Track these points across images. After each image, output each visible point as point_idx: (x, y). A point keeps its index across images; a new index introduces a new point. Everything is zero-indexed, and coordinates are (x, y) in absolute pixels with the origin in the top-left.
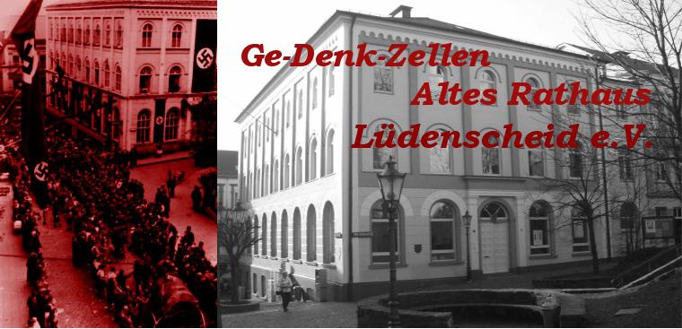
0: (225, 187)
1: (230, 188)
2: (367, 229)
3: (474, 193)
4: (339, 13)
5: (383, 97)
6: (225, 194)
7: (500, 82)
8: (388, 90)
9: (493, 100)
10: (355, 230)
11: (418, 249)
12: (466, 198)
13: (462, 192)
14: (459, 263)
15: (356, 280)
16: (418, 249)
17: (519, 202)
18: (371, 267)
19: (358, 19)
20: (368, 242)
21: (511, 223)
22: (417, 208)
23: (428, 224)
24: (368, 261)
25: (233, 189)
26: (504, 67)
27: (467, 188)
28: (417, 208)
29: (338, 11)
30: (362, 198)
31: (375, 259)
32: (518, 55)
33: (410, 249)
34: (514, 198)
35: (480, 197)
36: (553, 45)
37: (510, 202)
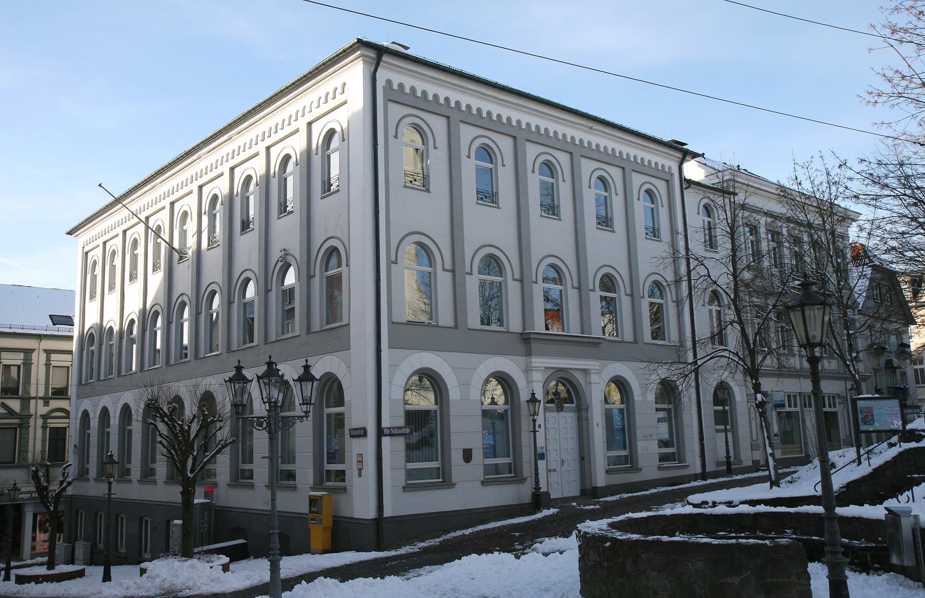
0: (34, 356)
1: (43, 356)
2: (401, 422)
3: (538, 362)
4: (362, 44)
5: (487, 211)
6: (34, 368)
7: (663, 206)
8: (553, 214)
9: (426, 188)
10: (385, 423)
11: (467, 455)
12: (528, 371)
13: (521, 360)
14: (518, 479)
15: (388, 513)
16: (467, 455)
17: (594, 378)
18: (405, 489)
19: (385, 58)
20: (400, 443)
21: (582, 411)
22: (465, 385)
23: (402, 414)
24: (402, 475)
25: (48, 359)
26: (444, 120)
27: (529, 354)
28: (465, 385)
29: (359, 41)
30: (394, 366)
31: (410, 474)
32: (544, 124)
33: (456, 457)
34: (585, 372)
35: (546, 368)
36: (667, 138)
37: (580, 377)
